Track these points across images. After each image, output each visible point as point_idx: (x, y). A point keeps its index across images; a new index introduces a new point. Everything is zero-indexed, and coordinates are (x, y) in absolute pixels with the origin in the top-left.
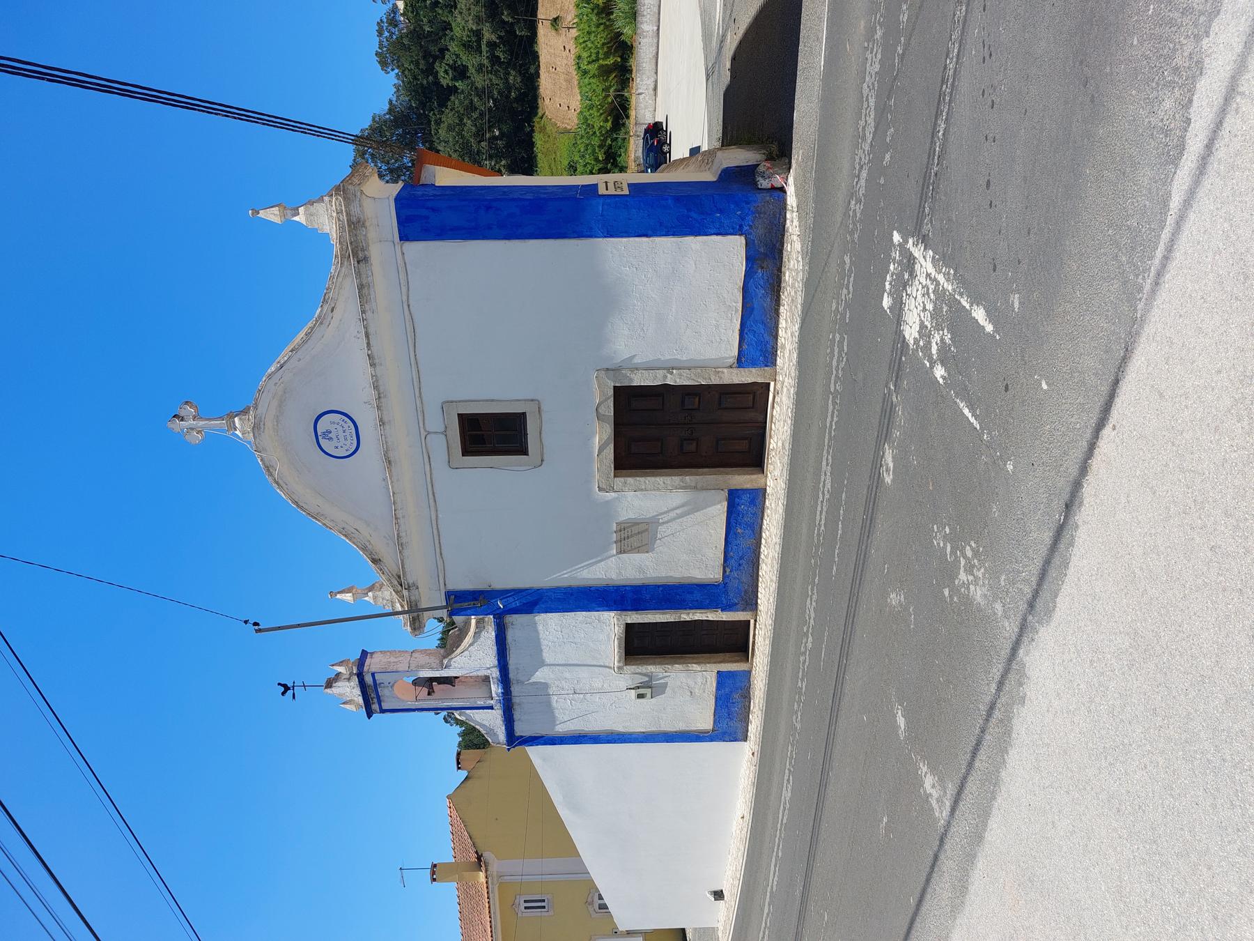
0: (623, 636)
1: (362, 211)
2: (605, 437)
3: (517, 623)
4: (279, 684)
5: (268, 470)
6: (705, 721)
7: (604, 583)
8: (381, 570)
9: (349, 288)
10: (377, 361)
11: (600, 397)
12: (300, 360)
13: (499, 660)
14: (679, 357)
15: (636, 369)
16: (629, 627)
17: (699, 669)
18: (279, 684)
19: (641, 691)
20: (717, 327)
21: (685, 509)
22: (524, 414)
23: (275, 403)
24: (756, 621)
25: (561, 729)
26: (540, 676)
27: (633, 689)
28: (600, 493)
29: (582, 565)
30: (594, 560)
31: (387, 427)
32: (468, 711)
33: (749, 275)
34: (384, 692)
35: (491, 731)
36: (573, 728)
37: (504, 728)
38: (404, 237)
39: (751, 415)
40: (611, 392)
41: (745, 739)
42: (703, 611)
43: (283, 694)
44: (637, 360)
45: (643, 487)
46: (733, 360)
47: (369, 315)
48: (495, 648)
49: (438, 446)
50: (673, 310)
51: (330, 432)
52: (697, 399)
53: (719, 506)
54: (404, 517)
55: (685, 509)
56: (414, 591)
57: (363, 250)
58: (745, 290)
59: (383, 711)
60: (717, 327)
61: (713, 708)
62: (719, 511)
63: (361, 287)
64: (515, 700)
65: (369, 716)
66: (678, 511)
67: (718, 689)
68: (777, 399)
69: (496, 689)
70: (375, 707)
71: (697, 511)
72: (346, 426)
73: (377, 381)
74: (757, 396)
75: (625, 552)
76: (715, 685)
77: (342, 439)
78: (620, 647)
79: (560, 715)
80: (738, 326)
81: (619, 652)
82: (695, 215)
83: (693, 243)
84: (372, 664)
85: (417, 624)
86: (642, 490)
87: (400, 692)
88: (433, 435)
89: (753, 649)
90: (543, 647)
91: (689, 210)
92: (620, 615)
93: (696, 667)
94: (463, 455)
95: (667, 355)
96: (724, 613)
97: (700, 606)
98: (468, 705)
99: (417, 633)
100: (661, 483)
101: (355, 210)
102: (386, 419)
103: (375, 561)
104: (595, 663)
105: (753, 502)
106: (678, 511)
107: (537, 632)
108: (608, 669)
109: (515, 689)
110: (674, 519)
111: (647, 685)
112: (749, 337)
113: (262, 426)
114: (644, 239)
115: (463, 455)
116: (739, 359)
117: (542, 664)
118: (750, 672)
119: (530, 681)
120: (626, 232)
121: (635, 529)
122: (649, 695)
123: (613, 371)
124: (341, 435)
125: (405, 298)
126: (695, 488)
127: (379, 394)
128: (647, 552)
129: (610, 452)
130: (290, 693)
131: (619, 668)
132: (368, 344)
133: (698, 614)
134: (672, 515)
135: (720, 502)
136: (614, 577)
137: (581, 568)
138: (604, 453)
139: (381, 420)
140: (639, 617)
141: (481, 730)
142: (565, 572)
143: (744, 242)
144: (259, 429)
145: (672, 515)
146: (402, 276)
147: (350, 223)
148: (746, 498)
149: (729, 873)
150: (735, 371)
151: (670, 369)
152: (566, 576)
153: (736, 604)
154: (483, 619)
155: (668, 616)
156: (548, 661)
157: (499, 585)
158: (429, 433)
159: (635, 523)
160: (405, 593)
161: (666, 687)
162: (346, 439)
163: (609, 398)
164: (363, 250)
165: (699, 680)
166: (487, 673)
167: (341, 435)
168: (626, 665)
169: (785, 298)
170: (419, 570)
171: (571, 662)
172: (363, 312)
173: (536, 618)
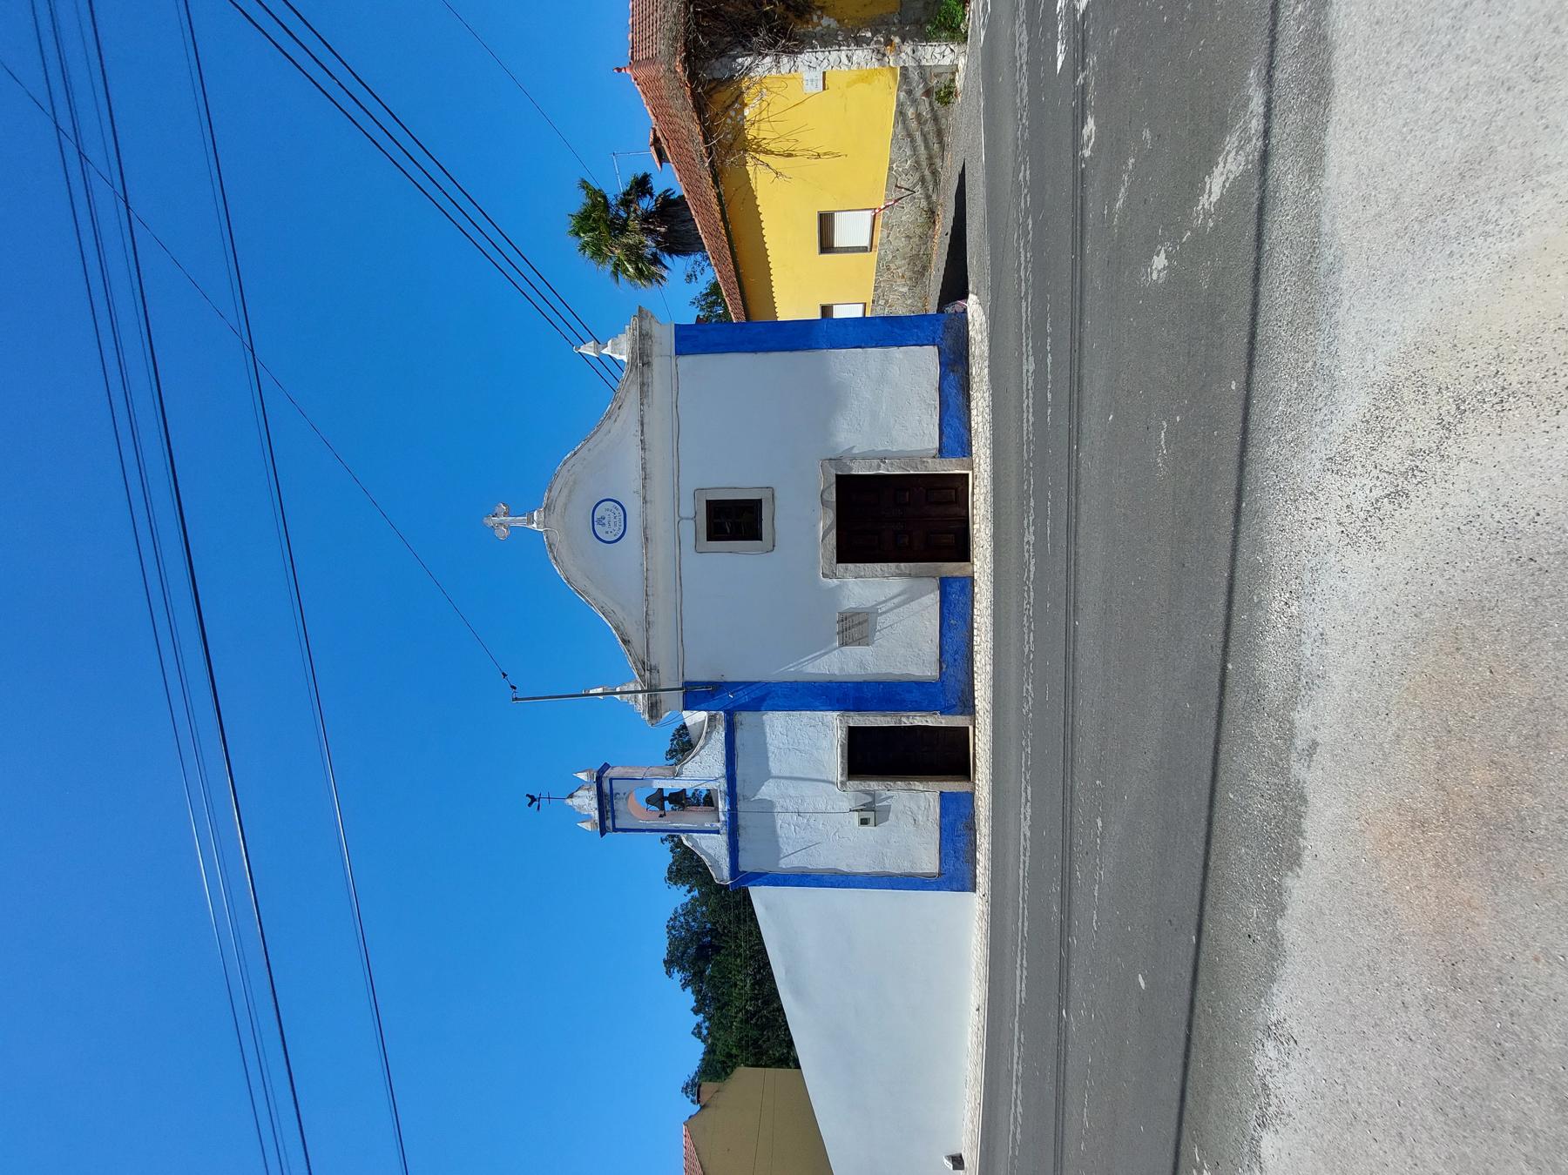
0: (846, 742)
1: (651, 327)
2: (829, 522)
3: (744, 718)
4: (528, 795)
5: (550, 547)
6: (928, 861)
7: (828, 679)
8: (629, 651)
9: (634, 392)
10: (647, 447)
11: (822, 485)
12: (589, 450)
13: (727, 771)
14: (890, 448)
15: (854, 459)
16: (854, 734)
17: (921, 788)
18: (528, 795)
19: (865, 815)
20: (920, 421)
21: (902, 598)
22: (760, 501)
23: (565, 492)
24: (974, 727)
25: (787, 864)
26: (768, 791)
27: (857, 811)
28: (825, 580)
29: (807, 658)
30: (818, 653)
31: (648, 505)
32: (695, 835)
33: (942, 378)
34: (619, 805)
35: (716, 862)
36: (796, 864)
37: (728, 860)
38: (679, 353)
39: (956, 510)
40: (834, 479)
41: (973, 888)
42: (924, 714)
43: (530, 805)
44: (855, 451)
45: (863, 574)
46: (934, 452)
47: (646, 407)
48: (724, 752)
49: (688, 529)
50: (884, 408)
51: (604, 519)
52: (907, 494)
53: (932, 595)
54: (653, 595)
55: (902, 598)
56: (655, 674)
57: (647, 356)
58: (941, 389)
59: (615, 830)
60: (920, 421)
61: (938, 843)
62: (932, 600)
63: (643, 384)
64: (741, 822)
65: (602, 834)
66: (896, 601)
67: (942, 816)
68: (976, 483)
69: (722, 805)
70: (609, 823)
71: (913, 601)
72: (617, 512)
73: (645, 463)
74: (957, 487)
75: (846, 645)
76: (938, 810)
77: (612, 524)
78: (842, 756)
79: (786, 848)
80: (938, 421)
81: (842, 762)
82: (896, 330)
83: (896, 353)
84: (610, 773)
85: (655, 711)
86: (861, 577)
87: (633, 809)
88: (685, 521)
89: (974, 760)
90: (770, 754)
91: (892, 326)
92: (843, 716)
93: (918, 785)
94: (708, 540)
95: (881, 446)
96: (943, 716)
97: (918, 708)
98: (695, 827)
99: (654, 722)
100: (879, 569)
101: (646, 325)
102: (648, 498)
103: (624, 641)
104: (819, 778)
105: (963, 589)
106: (896, 601)
107: (764, 734)
108: (831, 785)
109: (741, 806)
110: (891, 609)
111: (869, 807)
112: (947, 430)
113: (552, 508)
114: (860, 350)
115: (708, 540)
116: (940, 450)
117: (767, 775)
118: (973, 794)
119: (756, 798)
120: (846, 345)
121: (856, 620)
122: (872, 821)
123: (836, 460)
124: (612, 520)
125: (674, 400)
126: (910, 575)
127: (645, 475)
128: (868, 645)
129: (832, 538)
130: (535, 804)
131: (842, 783)
132: (642, 431)
133: (918, 718)
134: (890, 604)
135: (933, 591)
136: (836, 672)
137: (805, 661)
138: (827, 539)
139: (644, 498)
140: (861, 718)
141: (706, 860)
142: (791, 665)
143: (937, 351)
144: (549, 510)
145: (890, 604)
146: (674, 381)
147: (641, 334)
148: (956, 586)
149: (968, 1116)
150: (938, 460)
151: (883, 460)
152: (792, 669)
153: (955, 706)
154: (714, 716)
155: (889, 719)
156: (774, 772)
157: (729, 679)
158: (682, 519)
159: (855, 613)
160: (647, 673)
161: (889, 812)
162: (615, 525)
163: (832, 485)
164: (647, 356)
165: (923, 804)
166: (711, 785)
167: (612, 520)
168: (849, 780)
169: (975, 394)
170: (662, 655)
171: (795, 775)
172: (642, 404)
173: (764, 717)
